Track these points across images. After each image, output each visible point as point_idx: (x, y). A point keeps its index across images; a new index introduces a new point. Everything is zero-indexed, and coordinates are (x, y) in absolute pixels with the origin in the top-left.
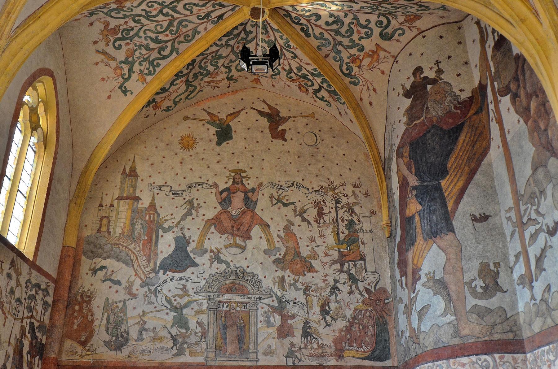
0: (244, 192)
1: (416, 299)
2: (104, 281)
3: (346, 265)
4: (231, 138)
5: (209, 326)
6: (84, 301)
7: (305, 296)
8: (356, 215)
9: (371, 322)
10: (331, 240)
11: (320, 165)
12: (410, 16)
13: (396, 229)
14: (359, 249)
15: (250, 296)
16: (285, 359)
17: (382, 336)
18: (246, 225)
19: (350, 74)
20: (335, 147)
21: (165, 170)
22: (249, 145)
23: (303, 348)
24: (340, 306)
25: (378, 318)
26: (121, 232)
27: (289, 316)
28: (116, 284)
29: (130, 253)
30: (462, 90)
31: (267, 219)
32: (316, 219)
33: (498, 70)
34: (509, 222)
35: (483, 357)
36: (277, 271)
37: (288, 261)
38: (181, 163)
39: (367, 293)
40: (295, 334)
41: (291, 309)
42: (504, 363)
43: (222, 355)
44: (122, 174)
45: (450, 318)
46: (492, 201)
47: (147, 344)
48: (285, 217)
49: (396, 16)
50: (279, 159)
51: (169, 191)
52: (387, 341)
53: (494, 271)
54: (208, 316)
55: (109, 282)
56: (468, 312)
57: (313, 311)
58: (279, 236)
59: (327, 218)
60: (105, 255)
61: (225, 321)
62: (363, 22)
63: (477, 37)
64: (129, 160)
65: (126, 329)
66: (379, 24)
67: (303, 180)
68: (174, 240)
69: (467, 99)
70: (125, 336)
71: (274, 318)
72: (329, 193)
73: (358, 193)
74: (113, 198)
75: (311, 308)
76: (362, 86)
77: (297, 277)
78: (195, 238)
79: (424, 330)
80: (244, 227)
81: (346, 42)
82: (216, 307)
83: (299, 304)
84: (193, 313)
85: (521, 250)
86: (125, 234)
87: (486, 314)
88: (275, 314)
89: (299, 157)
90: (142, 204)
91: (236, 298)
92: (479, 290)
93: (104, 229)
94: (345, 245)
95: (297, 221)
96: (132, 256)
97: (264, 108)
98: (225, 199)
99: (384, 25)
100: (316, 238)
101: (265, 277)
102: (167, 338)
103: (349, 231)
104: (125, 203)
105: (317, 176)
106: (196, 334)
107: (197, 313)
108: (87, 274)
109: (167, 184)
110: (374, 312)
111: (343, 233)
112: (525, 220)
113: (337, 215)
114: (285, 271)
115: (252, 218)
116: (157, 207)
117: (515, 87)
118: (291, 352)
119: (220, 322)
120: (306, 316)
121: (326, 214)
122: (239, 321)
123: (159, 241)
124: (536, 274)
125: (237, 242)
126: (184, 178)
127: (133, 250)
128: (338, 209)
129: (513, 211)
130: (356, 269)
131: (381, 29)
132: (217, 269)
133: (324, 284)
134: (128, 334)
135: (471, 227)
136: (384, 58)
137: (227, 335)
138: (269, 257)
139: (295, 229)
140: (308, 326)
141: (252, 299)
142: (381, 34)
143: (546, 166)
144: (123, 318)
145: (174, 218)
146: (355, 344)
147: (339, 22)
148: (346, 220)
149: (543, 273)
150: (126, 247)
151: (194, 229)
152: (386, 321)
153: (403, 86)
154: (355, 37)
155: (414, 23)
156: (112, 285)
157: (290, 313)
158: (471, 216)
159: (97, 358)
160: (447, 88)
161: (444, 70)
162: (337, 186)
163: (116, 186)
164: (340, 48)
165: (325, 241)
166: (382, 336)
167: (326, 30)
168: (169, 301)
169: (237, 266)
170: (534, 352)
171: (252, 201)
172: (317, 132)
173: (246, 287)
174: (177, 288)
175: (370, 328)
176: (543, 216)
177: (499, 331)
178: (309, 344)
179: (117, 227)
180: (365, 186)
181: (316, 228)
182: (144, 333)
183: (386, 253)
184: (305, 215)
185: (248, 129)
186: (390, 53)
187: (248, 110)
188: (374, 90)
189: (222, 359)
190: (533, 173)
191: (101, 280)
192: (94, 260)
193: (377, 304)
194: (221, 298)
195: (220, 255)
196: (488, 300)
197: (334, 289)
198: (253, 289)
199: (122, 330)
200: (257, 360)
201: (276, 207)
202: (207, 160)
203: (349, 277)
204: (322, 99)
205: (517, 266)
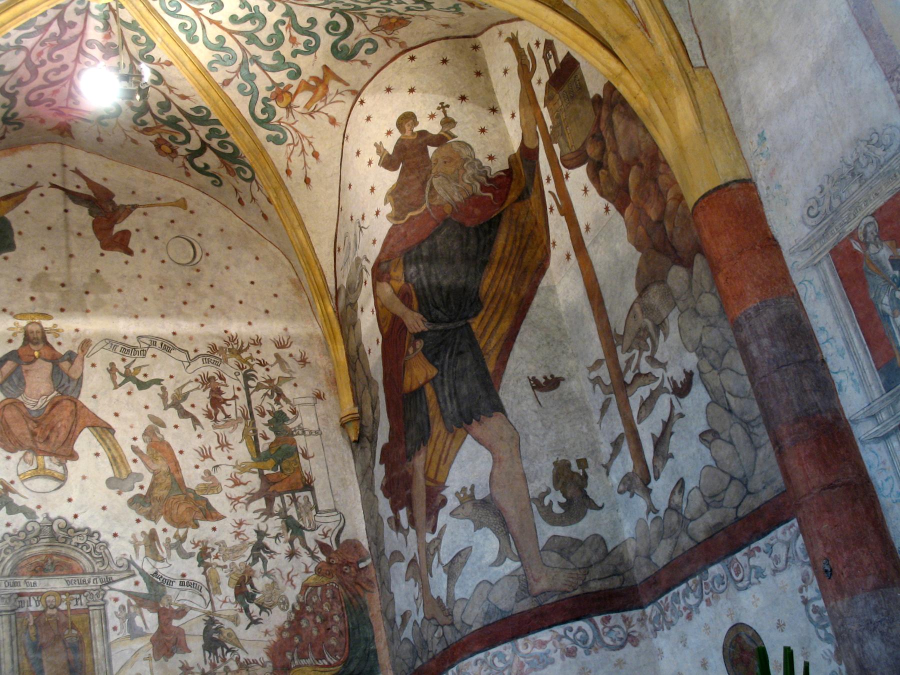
1: (440, 544)
3: (278, 500)
4: (11, 247)
7: (202, 569)
8: (287, 401)
9: (337, 608)
10: (242, 452)
11: (207, 303)
12: (389, 18)
13: (376, 423)
14: (299, 468)
15: (87, 577)
17: (359, 633)
19: (268, 121)
20: (232, 268)
22: (53, 262)
24: (274, 582)
25: (350, 599)
27: (173, 611)
30: (491, 158)
31: (106, 416)
32: (209, 411)
33: (561, 123)
34: (597, 387)
35: (575, 625)
36: (138, 521)
37: (160, 499)
39: (323, 553)
41: (177, 596)
42: (611, 629)
45: (511, 565)
46: (563, 352)
49: (364, 15)
52: (370, 640)
53: (578, 474)
56: (543, 550)
57: (222, 598)
58: (135, 449)
59: (230, 410)
61: (37, 636)
62: (303, 22)
63: (512, 63)
66: (332, 29)
69: (503, 173)
71: (143, 617)
72: (230, 360)
73: (286, 357)
75: (217, 591)
76: (291, 147)
77: (181, 532)
79: (462, 596)
80: (59, 433)
81: (267, 58)
82: (14, 608)
83: (192, 585)
85: (623, 431)
87: (572, 550)
88: (145, 611)
89: (161, 287)
91: (58, 584)
92: (557, 509)
94: (271, 463)
95: (171, 416)
97: (78, 187)
99: (341, 30)
103: (276, 433)
110: (341, 589)
111: (265, 438)
112: (629, 378)
113: (249, 402)
114: (156, 521)
117: (597, 151)
120: (209, 608)
121: (228, 402)
122: (67, 632)
124: (654, 467)
125: (47, 466)
128: (251, 390)
129: (605, 365)
130: (297, 508)
131: (332, 39)
132: (8, 525)
133: (238, 542)
135: (531, 401)
136: (337, 93)
137: (45, 664)
138: (120, 493)
139: (168, 435)
140: (214, 627)
141: (91, 584)
142: (334, 46)
143: (663, 281)
146: (310, 654)
147: (258, 19)
148: (269, 411)
149: (670, 462)
153: (379, 148)
154: (286, 50)
155: (395, 32)
157: (176, 604)
158: (530, 380)
160: (465, 153)
161: (456, 120)
162: (245, 345)
164: (254, 68)
165: (230, 455)
167: (231, 33)
169: (53, 516)
170: (659, 601)
171: (70, 380)
172: (193, 236)
175: (336, 618)
176: (663, 365)
177: (597, 577)
178: (220, 663)
184: (186, 405)
185: (49, 228)
186: (347, 84)
187: (46, 189)
188: (316, 155)
190: (640, 296)
193: (344, 573)
194: (23, 586)
195: (10, 495)
196: (574, 526)
197: (260, 549)
198: (91, 563)
201: (123, 390)
203: (287, 524)
204: (204, 170)
205: (618, 460)
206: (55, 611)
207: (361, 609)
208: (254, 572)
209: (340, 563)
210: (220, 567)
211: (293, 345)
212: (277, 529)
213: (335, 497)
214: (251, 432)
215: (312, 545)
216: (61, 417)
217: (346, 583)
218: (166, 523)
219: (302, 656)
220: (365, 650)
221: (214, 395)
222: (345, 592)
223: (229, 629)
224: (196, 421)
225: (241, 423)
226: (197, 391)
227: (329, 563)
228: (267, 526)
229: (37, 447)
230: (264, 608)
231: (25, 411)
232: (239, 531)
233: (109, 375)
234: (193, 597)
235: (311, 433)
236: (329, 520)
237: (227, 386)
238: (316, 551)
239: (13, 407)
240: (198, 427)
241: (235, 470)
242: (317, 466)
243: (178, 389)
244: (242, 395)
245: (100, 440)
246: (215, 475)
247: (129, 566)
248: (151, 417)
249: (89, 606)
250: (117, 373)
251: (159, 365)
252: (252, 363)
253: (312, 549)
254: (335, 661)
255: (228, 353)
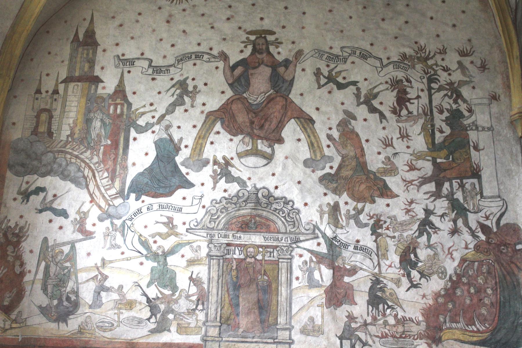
0: (270, 67)
2: (41, 211)
3: (447, 185)
5: (211, 285)
6: (9, 242)
7: (374, 237)
8: (465, 101)
9: (491, 282)
11: (402, 19)
14: (469, 158)
15: (280, 236)
16: (338, 341)
17: (510, 307)
18: (275, 119)
21: (142, 34)
23: (371, 324)
24: (436, 254)
25: (504, 275)
26: (68, 133)
27: (346, 269)
28: (60, 215)
29: (83, 167)
31: (309, 110)
32: (395, 108)
36: (325, 194)
37: (345, 179)
38: (168, 22)
39: (483, 233)
40: (357, 299)
43: (231, 333)
44: (72, 42)
47: (110, 312)
48: (340, 106)
50: (330, 11)
51: (147, 68)
54: (209, 268)
55: (49, 212)
57: (388, 263)
58: (330, 137)
59: (413, 108)
60: (43, 170)
64: (85, 20)
65: (75, 287)
67: (372, 44)
68: (154, 145)
70: (72, 299)
71: (320, 272)
72: (417, 66)
74: (57, 80)
75: (385, 256)
77: (360, 206)
78: (190, 141)
80: (271, 122)
82: (222, 254)
83: (364, 250)
84: (183, 262)
86: (76, 136)
88: (323, 267)
89: (365, 8)
90: (104, 88)
91: (257, 239)
93: (42, 129)
94: (445, 152)
95: (362, 111)
96: (86, 172)
98: (239, 78)
100: (394, 140)
101: (306, 204)
102: (140, 303)
103: (451, 128)
104: (76, 87)
105: (396, 38)
106: (188, 297)
107: (191, 262)
108: (15, 199)
109: (144, 57)
111: (441, 132)
113: (431, 101)
114: (340, 196)
115: (285, 108)
116: (127, 92)
118: (349, 330)
119: (228, 277)
120: (376, 270)
121: (411, 101)
122: (260, 277)
123: (131, 147)
125: (259, 147)
126: (173, 45)
127: (88, 161)
128: (433, 91)
130: (463, 192)
132: (225, 191)
133: (407, 217)
134: (77, 296)
137: (241, 300)
138: (313, 171)
139: (358, 126)
140: (379, 286)
141: (283, 241)
144: (69, 271)
145: (155, 110)
148: (447, 110)
150: (77, 157)
151: (187, 126)
152: (518, 281)
156: (53, 217)
157: (348, 264)
159: (28, 333)
162: (432, 54)
163: (63, 62)
165: (409, 145)
166: (510, 307)
168: (144, 243)
169: (258, 186)
171: (284, 81)
173: (273, 221)
174: (157, 222)
175: (489, 291)
178: (381, 317)
179: (63, 126)
180: (481, 53)
181: (395, 124)
182: (103, 294)
183: (518, 165)
184: (375, 103)
189: (231, 339)
191: (36, 209)
192: (26, 178)
193: (501, 252)
195: (230, 168)
199: (68, 289)
200: (291, 341)
201: (325, 90)
202: (210, 16)
203: (453, 205)
206: (253, 260)
207: (514, 285)
208: (419, 243)
209: (498, 243)
210: (389, 237)
211: (475, 54)
212: (443, 209)
213: (500, 186)
214: (429, 126)
215: (473, 225)
216: (274, 110)
217: (502, 262)
218: (348, 198)
219: (453, 320)
220: (514, 323)
221: (400, 95)
222: (501, 269)
223: (391, 289)
224: (382, 116)
225: (421, 118)
226: (388, 91)
227: (488, 242)
228: (435, 206)
229: (254, 132)
230: (424, 275)
231: (247, 104)
232: (409, 208)
233: (315, 78)
234: (364, 260)
235: (483, 129)
236: (492, 204)
237: (412, 87)
238: (477, 231)
239: (239, 101)
240: (384, 121)
241: (412, 157)
242: (486, 158)
243: (370, 89)
244: (424, 96)
245: (303, 129)
246: (395, 161)
247: (314, 230)
248: (346, 112)
249: (279, 259)
250: (321, 76)
251: (356, 70)
252: (436, 69)
253: (474, 228)
254: (484, 328)
255: (416, 60)
